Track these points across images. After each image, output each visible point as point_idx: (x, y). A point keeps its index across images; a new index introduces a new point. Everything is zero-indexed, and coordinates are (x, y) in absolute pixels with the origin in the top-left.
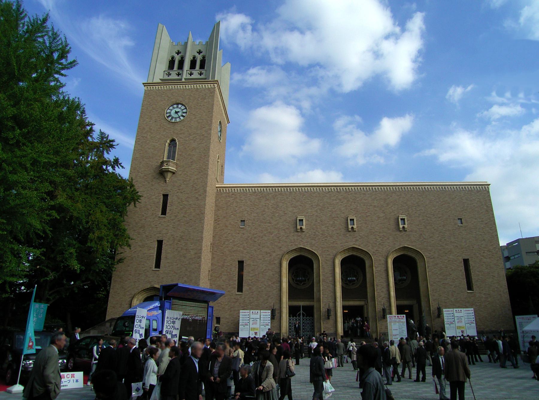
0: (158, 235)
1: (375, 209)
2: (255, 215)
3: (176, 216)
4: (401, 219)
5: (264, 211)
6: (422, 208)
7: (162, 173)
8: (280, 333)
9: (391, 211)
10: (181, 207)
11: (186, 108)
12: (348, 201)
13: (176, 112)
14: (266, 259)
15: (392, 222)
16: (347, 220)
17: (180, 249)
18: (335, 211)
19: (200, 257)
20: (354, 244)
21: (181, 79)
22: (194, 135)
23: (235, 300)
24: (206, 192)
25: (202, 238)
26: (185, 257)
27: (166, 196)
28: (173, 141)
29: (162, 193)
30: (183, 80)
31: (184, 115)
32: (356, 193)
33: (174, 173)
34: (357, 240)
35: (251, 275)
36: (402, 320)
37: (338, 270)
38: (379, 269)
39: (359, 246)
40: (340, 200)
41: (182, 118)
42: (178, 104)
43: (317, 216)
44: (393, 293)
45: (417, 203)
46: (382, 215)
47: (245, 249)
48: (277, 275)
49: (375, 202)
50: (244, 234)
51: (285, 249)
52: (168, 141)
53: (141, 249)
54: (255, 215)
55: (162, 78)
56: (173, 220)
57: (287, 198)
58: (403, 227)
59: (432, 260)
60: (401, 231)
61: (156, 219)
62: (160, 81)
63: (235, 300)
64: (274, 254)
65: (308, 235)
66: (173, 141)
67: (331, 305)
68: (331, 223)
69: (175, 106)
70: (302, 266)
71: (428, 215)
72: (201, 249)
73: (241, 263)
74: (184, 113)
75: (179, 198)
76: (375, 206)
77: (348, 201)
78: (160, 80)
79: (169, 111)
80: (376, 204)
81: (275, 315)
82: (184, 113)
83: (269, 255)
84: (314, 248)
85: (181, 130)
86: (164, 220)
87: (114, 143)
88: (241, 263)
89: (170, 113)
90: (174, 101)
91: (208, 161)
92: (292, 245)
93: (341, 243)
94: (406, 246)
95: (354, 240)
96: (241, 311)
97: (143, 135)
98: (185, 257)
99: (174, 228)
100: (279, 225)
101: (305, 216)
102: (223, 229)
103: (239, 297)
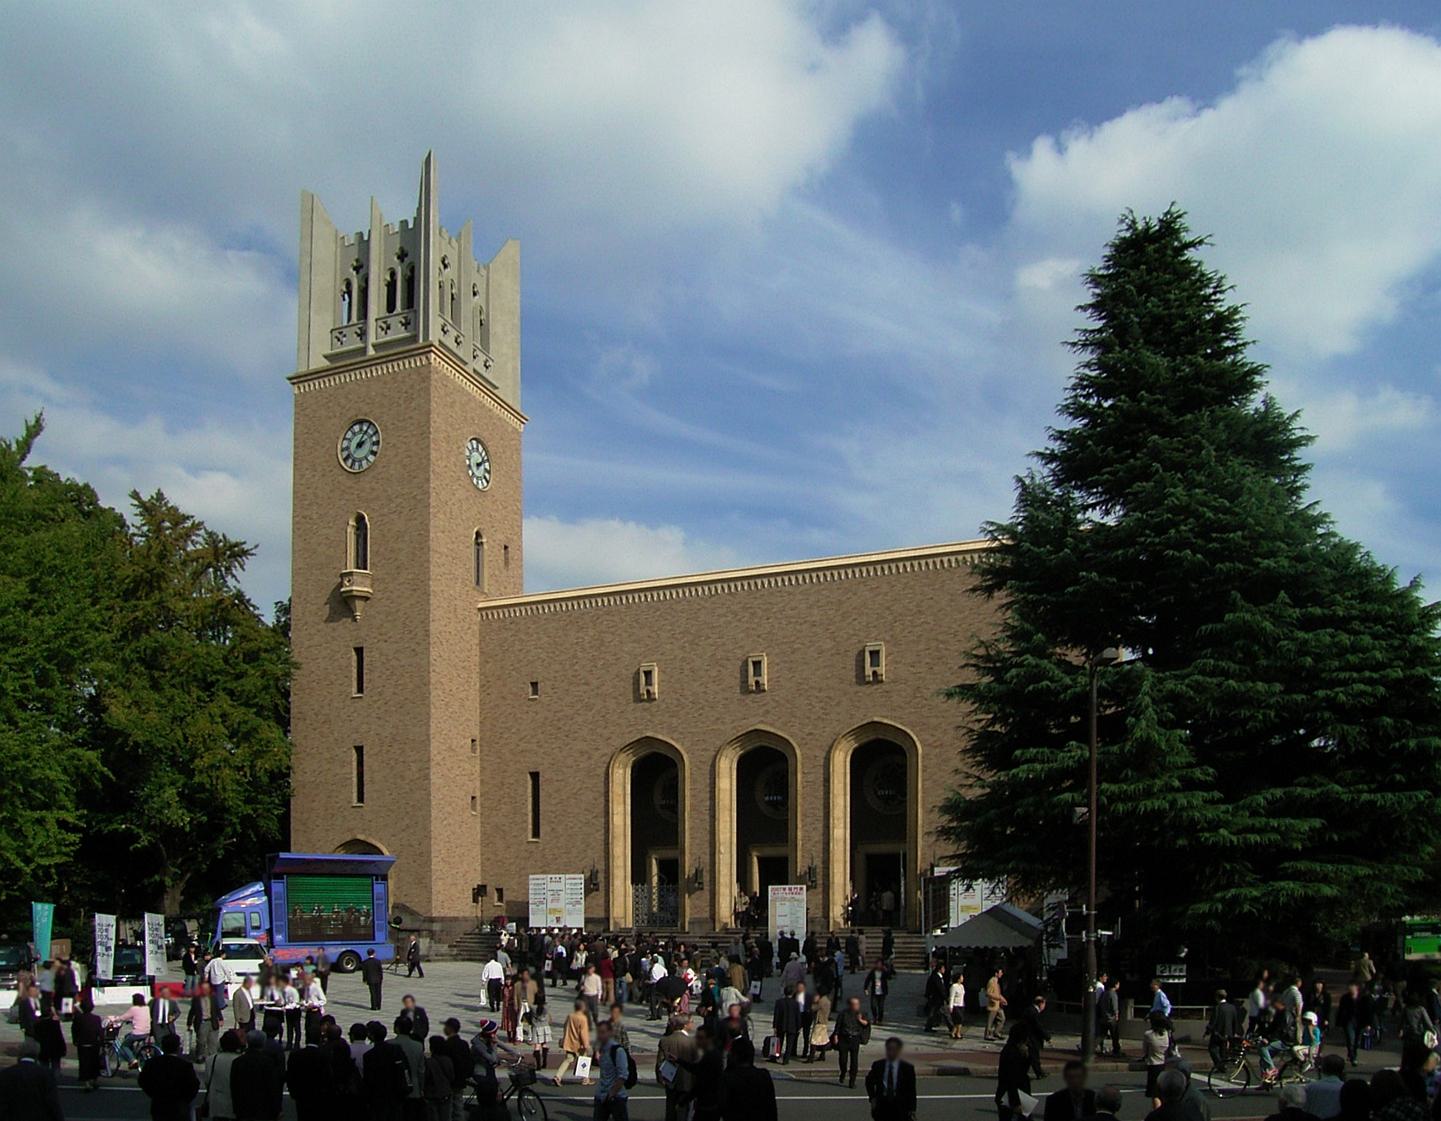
0: (355, 736)
1: (814, 629)
2: (558, 667)
3: (380, 694)
4: (871, 653)
5: (575, 656)
6: (930, 619)
7: (343, 604)
8: (608, 919)
9: (851, 632)
10: (388, 673)
11: (376, 432)
12: (753, 614)
13: (360, 445)
14: (582, 766)
15: (851, 663)
16: (747, 665)
17: (392, 763)
18: (724, 644)
19: (427, 777)
20: (762, 722)
21: (364, 350)
22: (399, 500)
23: (526, 855)
24: (428, 636)
25: (428, 735)
26: (403, 778)
27: (359, 651)
28: (360, 519)
29: (353, 644)
30: (371, 352)
31: (375, 448)
32: (772, 594)
33: (366, 599)
34: (768, 712)
35: (554, 802)
36: (797, 897)
38: (811, 778)
39: (771, 725)
41: (371, 458)
42: (361, 422)
43: (683, 659)
44: (841, 832)
45: (918, 606)
46: (829, 644)
47: (541, 746)
48: (602, 799)
49: (816, 612)
50: (537, 713)
51: (619, 743)
52: (352, 522)
53: (328, 766)
54: (558, 667)
55: (328, 352)
56: (375, 702)
57: (622, 621)
59: (937, 750)
60: (869, 683)
61: (348, 702)
62: (326, 363)
63: (526, 855)
64: (596, 755)
66: (360, 519)
67: (707, 859)
69: (356, 428)
70: (657, 776)
71: (940, 637)
72: (429, 760)
73: (535, 776)
74: (374, 444)
75: (381, 654)
77: (753, 614)
78: (326, 357)
79: (345, 443)
81: (596, 884)
82: (374, 444)
83: (586, 756)
84: (675, 735)
85: (373, 489)
86: (359, 704)
87: (246, 547)
89: (347, 448)
90: (352, 414)
91: (428, 561)
92: (630, 732)
93: (733, 722)
94: (876, 719)
95: (761, 711)
96: (531, 877)
97: (306, 513)
98: (403, 778)
99: (379, 718)
100: (604, 688)
101: (658, 661)
102: (497, 706)
103: (533, 846)
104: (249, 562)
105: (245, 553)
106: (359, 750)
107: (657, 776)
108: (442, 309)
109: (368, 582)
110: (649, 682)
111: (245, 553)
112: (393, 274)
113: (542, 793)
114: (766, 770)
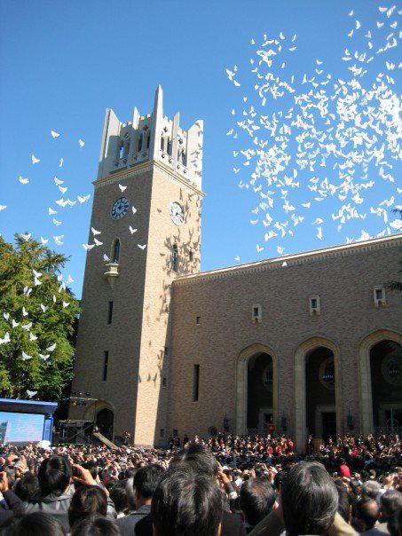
13: (120, 208)
27: (111, 303)
28: (117, 242)
34: (320, 327)
37: (300, 369)
40: (302, 276)
58: (380, 302)
65: (265, 326)
66: (117, 242)
68: (291, 307)
70: (260, 367)
73: (197, 367)
76: (344, 278)
80: (346, 274)
87: (64, 257)
88: (197, 367)
104: (66, 263)
105: (63, 260)
106: (107, 353)
107: (260, 367)
108: (162, 147)
109: (116, 268)
110: (256, 313)
111: (63, 260)
112: (141, 136)
113: (200, 376)
114: (319, 361)
